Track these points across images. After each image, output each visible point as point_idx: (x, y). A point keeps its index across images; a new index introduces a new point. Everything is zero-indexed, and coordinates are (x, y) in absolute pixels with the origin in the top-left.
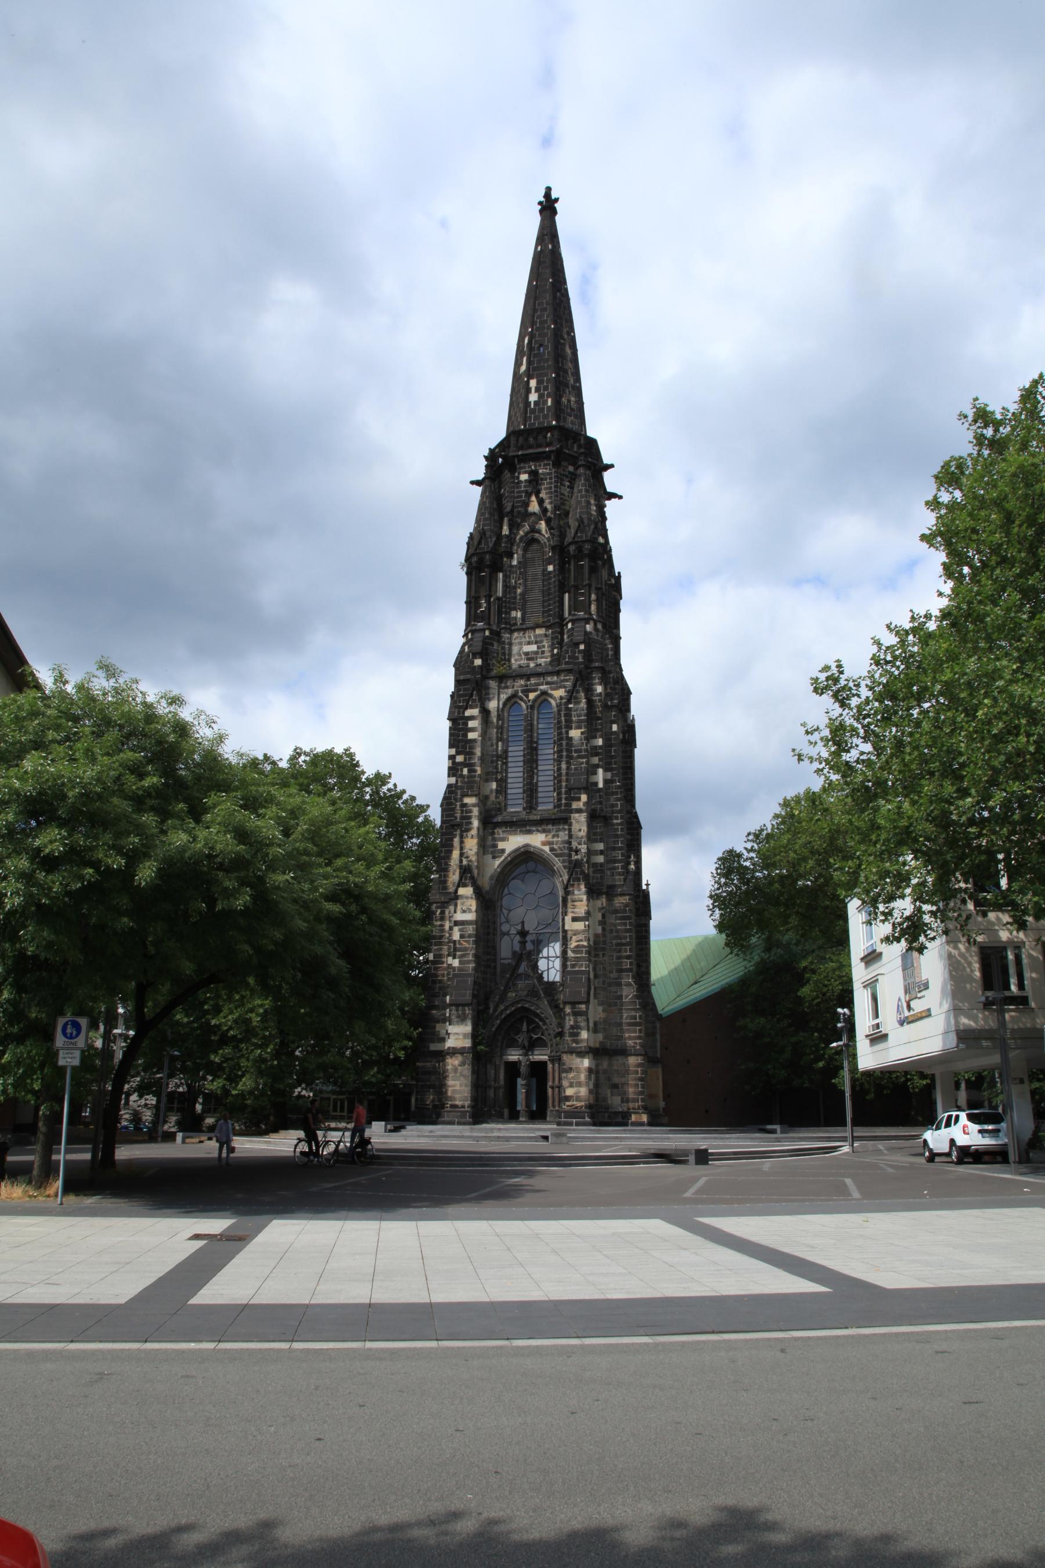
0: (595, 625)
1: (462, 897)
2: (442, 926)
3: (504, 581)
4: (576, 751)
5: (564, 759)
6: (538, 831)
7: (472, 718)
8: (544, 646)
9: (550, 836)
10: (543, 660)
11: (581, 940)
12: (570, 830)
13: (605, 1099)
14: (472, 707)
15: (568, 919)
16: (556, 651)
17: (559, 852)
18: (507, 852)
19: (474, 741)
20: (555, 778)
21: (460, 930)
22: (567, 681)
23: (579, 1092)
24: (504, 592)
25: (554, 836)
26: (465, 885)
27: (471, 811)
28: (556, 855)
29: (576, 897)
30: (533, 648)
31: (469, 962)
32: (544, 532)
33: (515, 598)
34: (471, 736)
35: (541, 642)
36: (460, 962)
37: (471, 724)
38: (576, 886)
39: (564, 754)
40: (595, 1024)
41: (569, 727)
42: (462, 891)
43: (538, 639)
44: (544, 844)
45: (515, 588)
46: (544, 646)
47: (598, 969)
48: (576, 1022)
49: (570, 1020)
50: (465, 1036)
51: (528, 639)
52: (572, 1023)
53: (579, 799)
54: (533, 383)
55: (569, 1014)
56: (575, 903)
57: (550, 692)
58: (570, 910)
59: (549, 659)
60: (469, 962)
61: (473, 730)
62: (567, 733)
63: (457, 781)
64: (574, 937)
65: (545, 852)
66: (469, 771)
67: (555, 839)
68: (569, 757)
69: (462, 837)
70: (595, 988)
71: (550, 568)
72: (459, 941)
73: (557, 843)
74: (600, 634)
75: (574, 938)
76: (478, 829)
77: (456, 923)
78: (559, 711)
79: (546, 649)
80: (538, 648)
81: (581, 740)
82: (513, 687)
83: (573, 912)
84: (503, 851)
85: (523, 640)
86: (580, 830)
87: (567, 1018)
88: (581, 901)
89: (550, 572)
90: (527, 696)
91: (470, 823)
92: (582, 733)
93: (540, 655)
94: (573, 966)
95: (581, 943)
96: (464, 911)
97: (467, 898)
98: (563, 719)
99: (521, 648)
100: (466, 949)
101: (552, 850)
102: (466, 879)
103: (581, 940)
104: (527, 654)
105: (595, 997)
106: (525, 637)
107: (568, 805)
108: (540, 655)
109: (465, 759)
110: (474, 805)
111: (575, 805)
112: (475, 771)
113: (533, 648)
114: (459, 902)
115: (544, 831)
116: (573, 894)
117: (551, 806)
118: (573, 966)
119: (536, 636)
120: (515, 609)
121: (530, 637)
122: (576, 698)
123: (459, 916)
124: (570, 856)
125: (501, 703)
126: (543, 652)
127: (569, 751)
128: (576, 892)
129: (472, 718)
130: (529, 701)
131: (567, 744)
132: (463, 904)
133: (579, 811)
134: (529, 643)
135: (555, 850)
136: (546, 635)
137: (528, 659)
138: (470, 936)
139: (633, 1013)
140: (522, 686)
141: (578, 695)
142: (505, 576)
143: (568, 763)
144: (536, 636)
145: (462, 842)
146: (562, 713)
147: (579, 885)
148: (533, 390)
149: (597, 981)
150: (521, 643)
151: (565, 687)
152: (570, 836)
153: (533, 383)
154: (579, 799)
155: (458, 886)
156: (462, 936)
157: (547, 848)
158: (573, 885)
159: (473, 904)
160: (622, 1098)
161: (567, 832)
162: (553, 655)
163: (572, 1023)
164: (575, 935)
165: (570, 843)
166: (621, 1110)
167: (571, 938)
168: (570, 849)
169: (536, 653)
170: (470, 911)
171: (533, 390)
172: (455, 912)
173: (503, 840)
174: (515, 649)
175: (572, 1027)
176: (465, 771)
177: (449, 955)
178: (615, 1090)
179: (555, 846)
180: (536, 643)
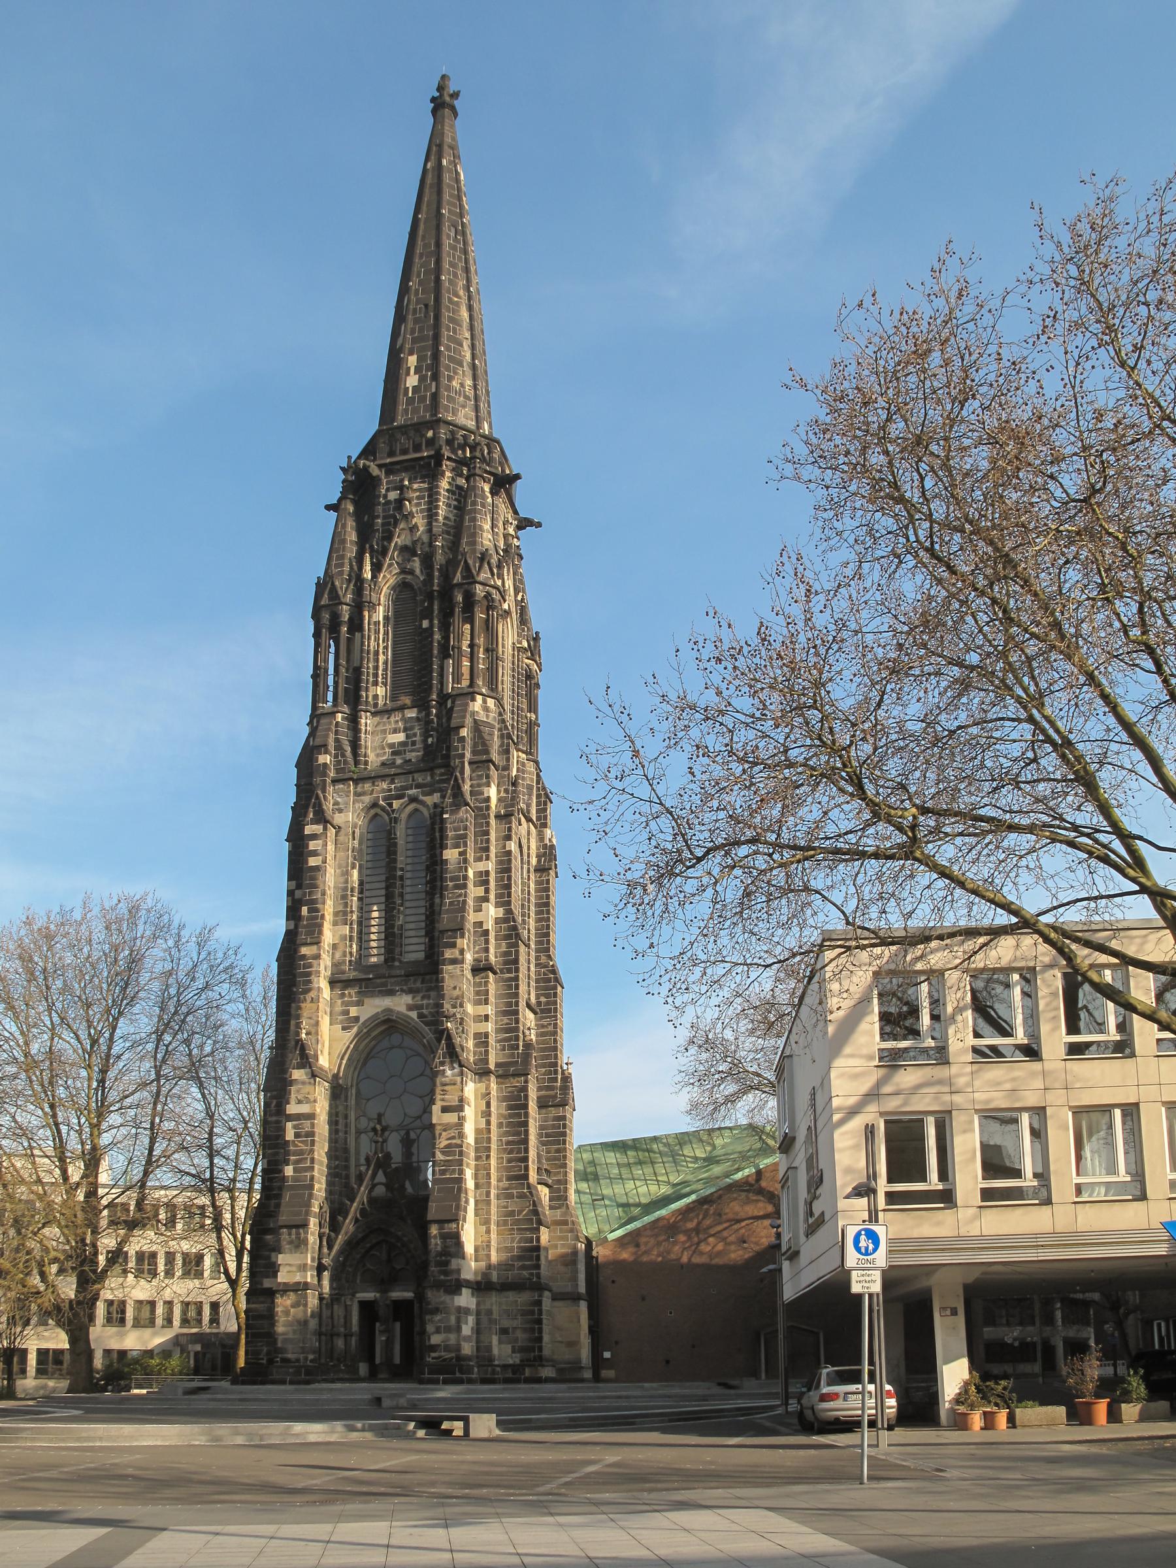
0: (485, 702)
10: (414, 754)
13: (489, 1348)
16: (430, 740)
18: (362, 1020)
20: (427, 917)
32: (418, 572)
35: (412, 728)
44: (410, 1008)
57: (421, 797)
65: (413, 1019)
74: (492, 715)
104: (391, 746)
106: (390, 723)
117: (421, 956)
130: (393, 811)
134: (395, 731)
157: (414, 1015)
162: (426, 747)
166: (511, 1362)
178: (503, 1336)
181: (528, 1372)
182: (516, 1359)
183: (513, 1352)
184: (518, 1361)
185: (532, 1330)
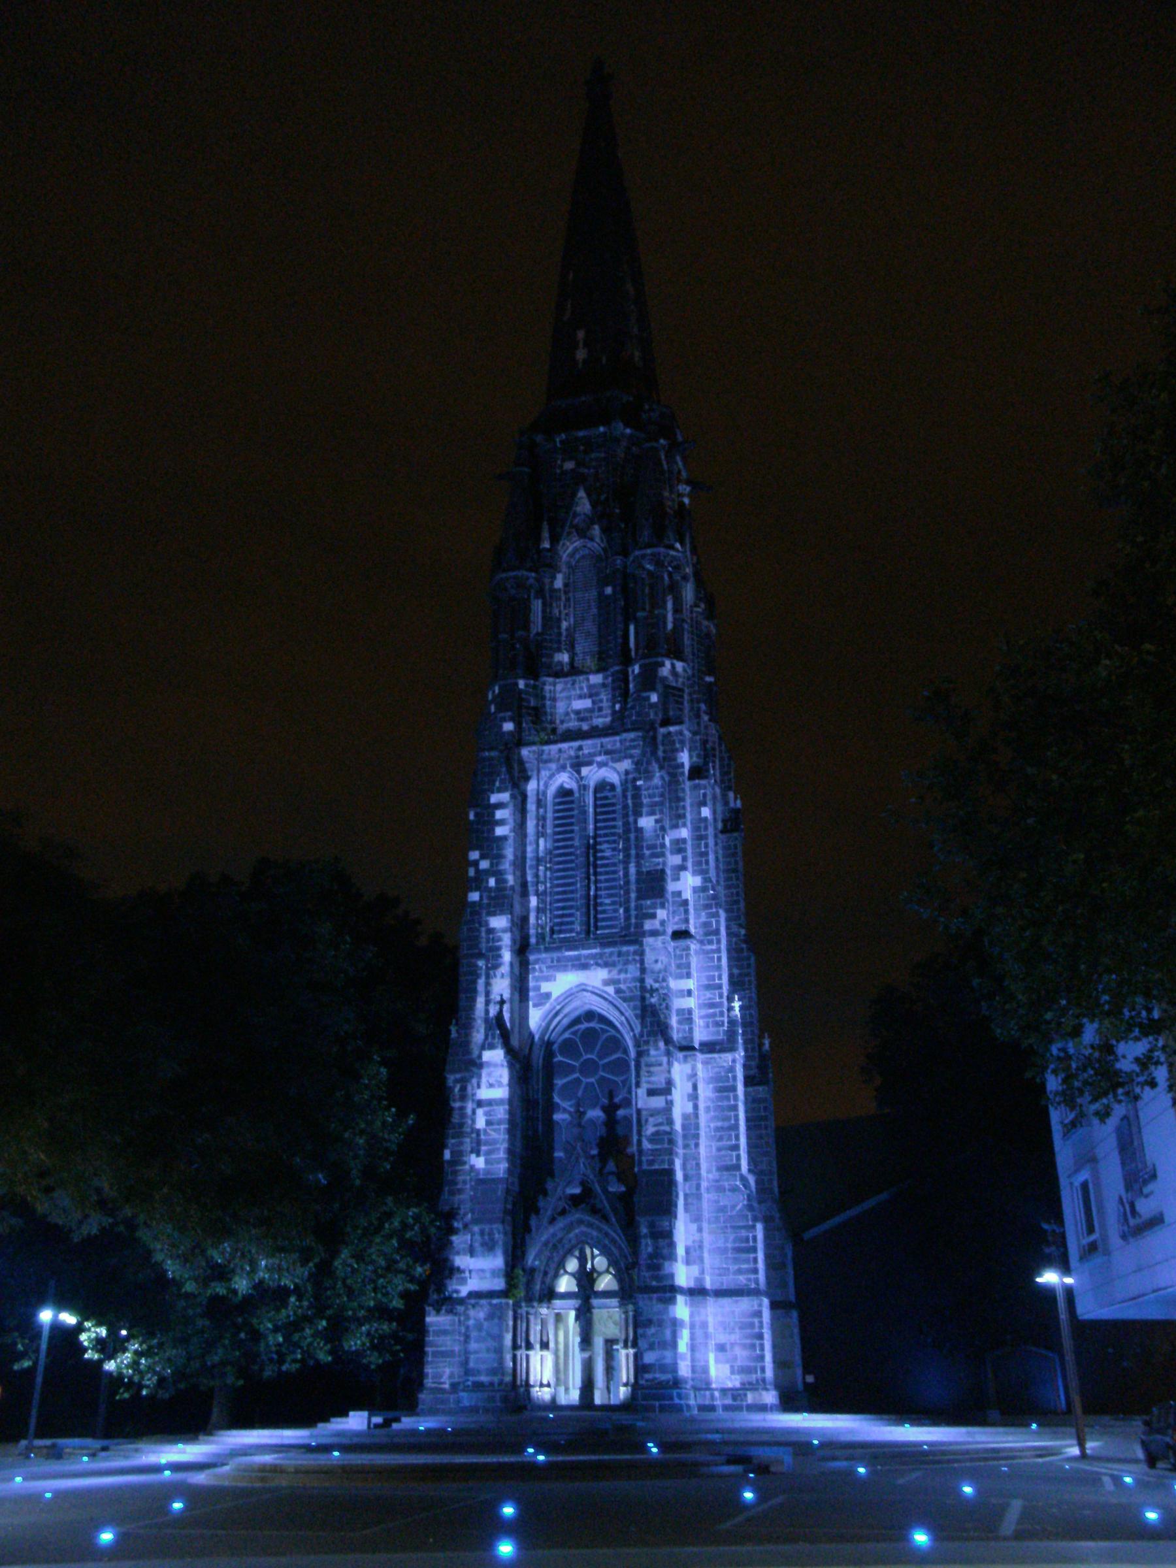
1: (488, 1064)
2: (462, 1108)
3: (544, 611)
4: (648, 848)
5: (633, 859)
6: (598, 964)
7: (500, 805)
8: (601, 701)
9: (615, 972)
11: (661, 1124)
12: (642, 962)
13: (706, 1370)
14: (500, 790)
15: (641, 1092)
17: (628, 994)
18: (554, 995)
19: (505, 838)
21: (486, 1114)
22: (634, 747)
23: (664, 1358)
24: (544, 626)
25: (620, 972)
26: (492, 1047)
27: (500, 939)
28: (625, 1000)
29: (653, 1060)
30: (587, 703)
31: (498, 1161)
33: (560, 634)
34: (500, 831)
35: (597, 694)
36: (487, 1162)
37: (499, 814)
38: (651, 1043)
39: (633, 852)
40: (688, 1251)
41: (638, 814)
42: (487, 1055)
43: (594, 691)
44: (607, 983)
45: (559, 620)
46: (601, 701)
47: (689, 1167)
48: (656, 1248)
49: (647, 1245)
50: (494, 1273)
51: (578, 692)
52: (650, 1249)
53: (654, 916)
54: (581, 334)
55: (645, 1236)
56: (652, 1069)
58: (643, 1079)
59: (608, 719)
60: (498, 1161)
61: (502, 822)
62: (636, 822)
63: (481, 897)
64: (651, 1120)
65: (609, 995)
66: (497, 882)
67: (622, 976)
68: (639, 856)
69: (488, 977)
70: (686, 1196)
71: (609, 590)
72: (485, 1130)
73: (625, 981)
75: (651, 1120)
76: (511, 964)
77: (480, 1104)
78: (625, 791)
79: (605, 704)
80: (594, 702)
81: (655, 831)
82: (559, 759)
83: (649, 1082)
84: (548, 995)
85: (573, 693)
86: (656, 961)
87: (643, 1241)
88: (660, 1065)
89: (608, 597)
90: (579, 772)
91: (500, 956)
92: (657, 821)
93: (596, 714)
94: (651, 1162)
95: (662, 1128)
96: (491, 1086)
97: (496, 1065)
98: (630, 802)
99: (569, 705)
100: (495, 1142)
101: (618, 991)
102: (493, 1038)
103: (661, 1124)
104: (578, 712)
105: (686, 1210)
107: (639, 926)
108: (596, 714)
109: (492, 864)
110: (504, 931)
111: (648, 925)
112: (505, 881)
113: (587, 703)
114: (484, 1072)
115: (606, 965)
116: (648, 1055)
118: (651, 1162)
119: (590, 687)
120: (559, 650)
121: (581, 688)
122: (647, 771)
123: (484, 1093)
124: (643, 999)
125: (542, 783)
126: (600, 709)
127: (639, 847)
128: (652, 1052)
129: (500, 805)
131: (637, 838)
132: (489, 1075)
133: (654, 933)
134: (580, 697)
135: (624, 992)
136: (604, 685)
137: (582, 720)
138: (500, 1122)
139: (744, 1233)
140: (570, 758)
141: (650, 768)
142: (544, 604)
143: (638, 865)
144: (590, 687)
145: (488, 984)
146: (629, 794)
147: (656, 1041)
148: (581, 344)
149: (688, 1184)
150: (569, 698)
151: (631, 757)
152: (643, 970)
153: (581, 334)
154: (654, 916)
155: (483, 1048)
156: (489, 1123)
157: (610, 990)
158: (647, 1042)
159: (504, 1075)
160: (732, 1367)
161: (638, 965)
162: (614, 713)
163: (650, 1249)
164: (652, 1115)
165: (642, 981)
166: (730, 1385)
167: (647, 1121)
168: (643, 989)
169: (591, 710)
170: (500, 1085)
171: (581, 344)
172: (479, 1086)
173: (548, 979)
174: (561, 707)
175: (651, 1256)
176: (492, 882)
177: (472, 1152)
178: (720, 1354)
179: (622, 986)
180: (591, 696)
181: (750, 1398)
182: (734, 1382)
183: (732, 1372)
184: (737, 1384)
185: (753, 1346)
